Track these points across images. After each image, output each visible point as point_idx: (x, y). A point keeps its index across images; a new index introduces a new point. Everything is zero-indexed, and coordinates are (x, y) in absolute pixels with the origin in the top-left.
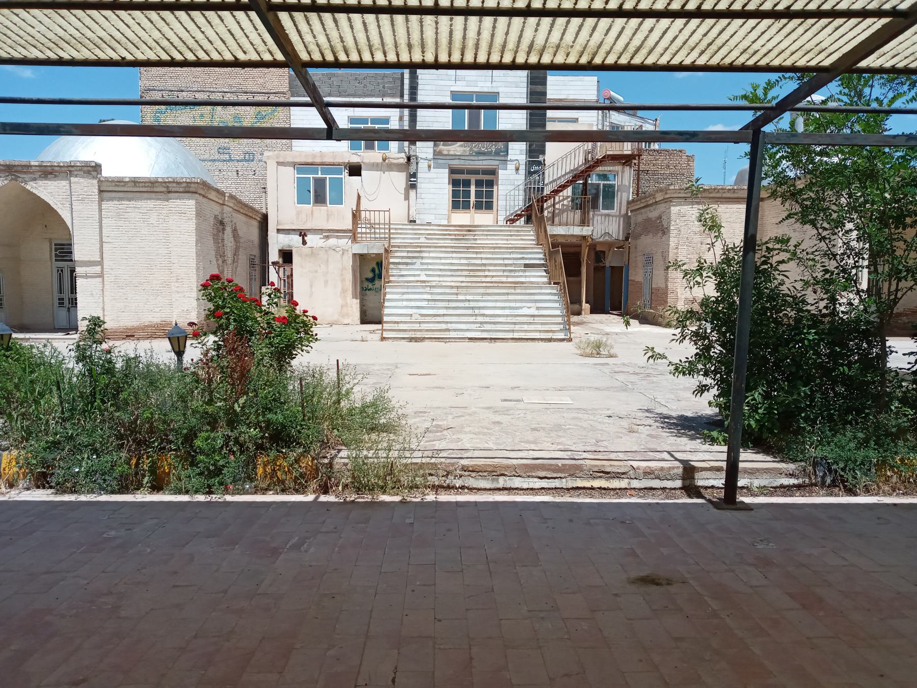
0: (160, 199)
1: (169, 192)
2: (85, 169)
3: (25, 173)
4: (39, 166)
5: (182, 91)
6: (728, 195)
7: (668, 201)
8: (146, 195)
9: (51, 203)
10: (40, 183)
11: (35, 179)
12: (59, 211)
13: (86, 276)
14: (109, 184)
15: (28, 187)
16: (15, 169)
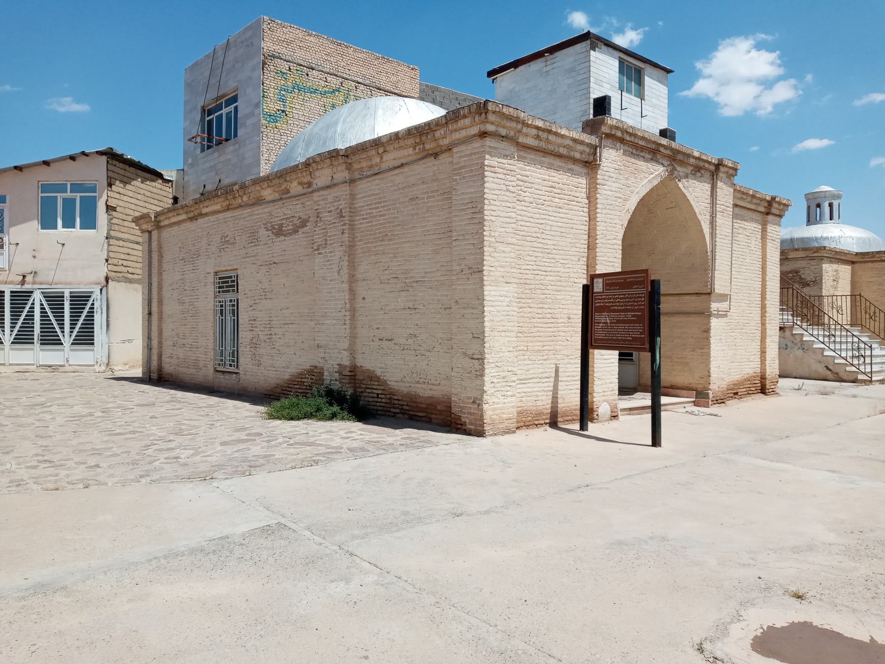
0: (756, 221)
1: (768, 214)
2: (731, 171)
3: (682, 163)
4: (699, 159)
5: (313, 69)
6: (843, 258)
7: (821, 258)
8: (750, 213)
9: (696, 211)
10: (691, 181)
11: (686, 177)
12: (702, 223)
13: (718, 316)
14: (739, 195)
15: (681, 185)
16: (680, 157)
